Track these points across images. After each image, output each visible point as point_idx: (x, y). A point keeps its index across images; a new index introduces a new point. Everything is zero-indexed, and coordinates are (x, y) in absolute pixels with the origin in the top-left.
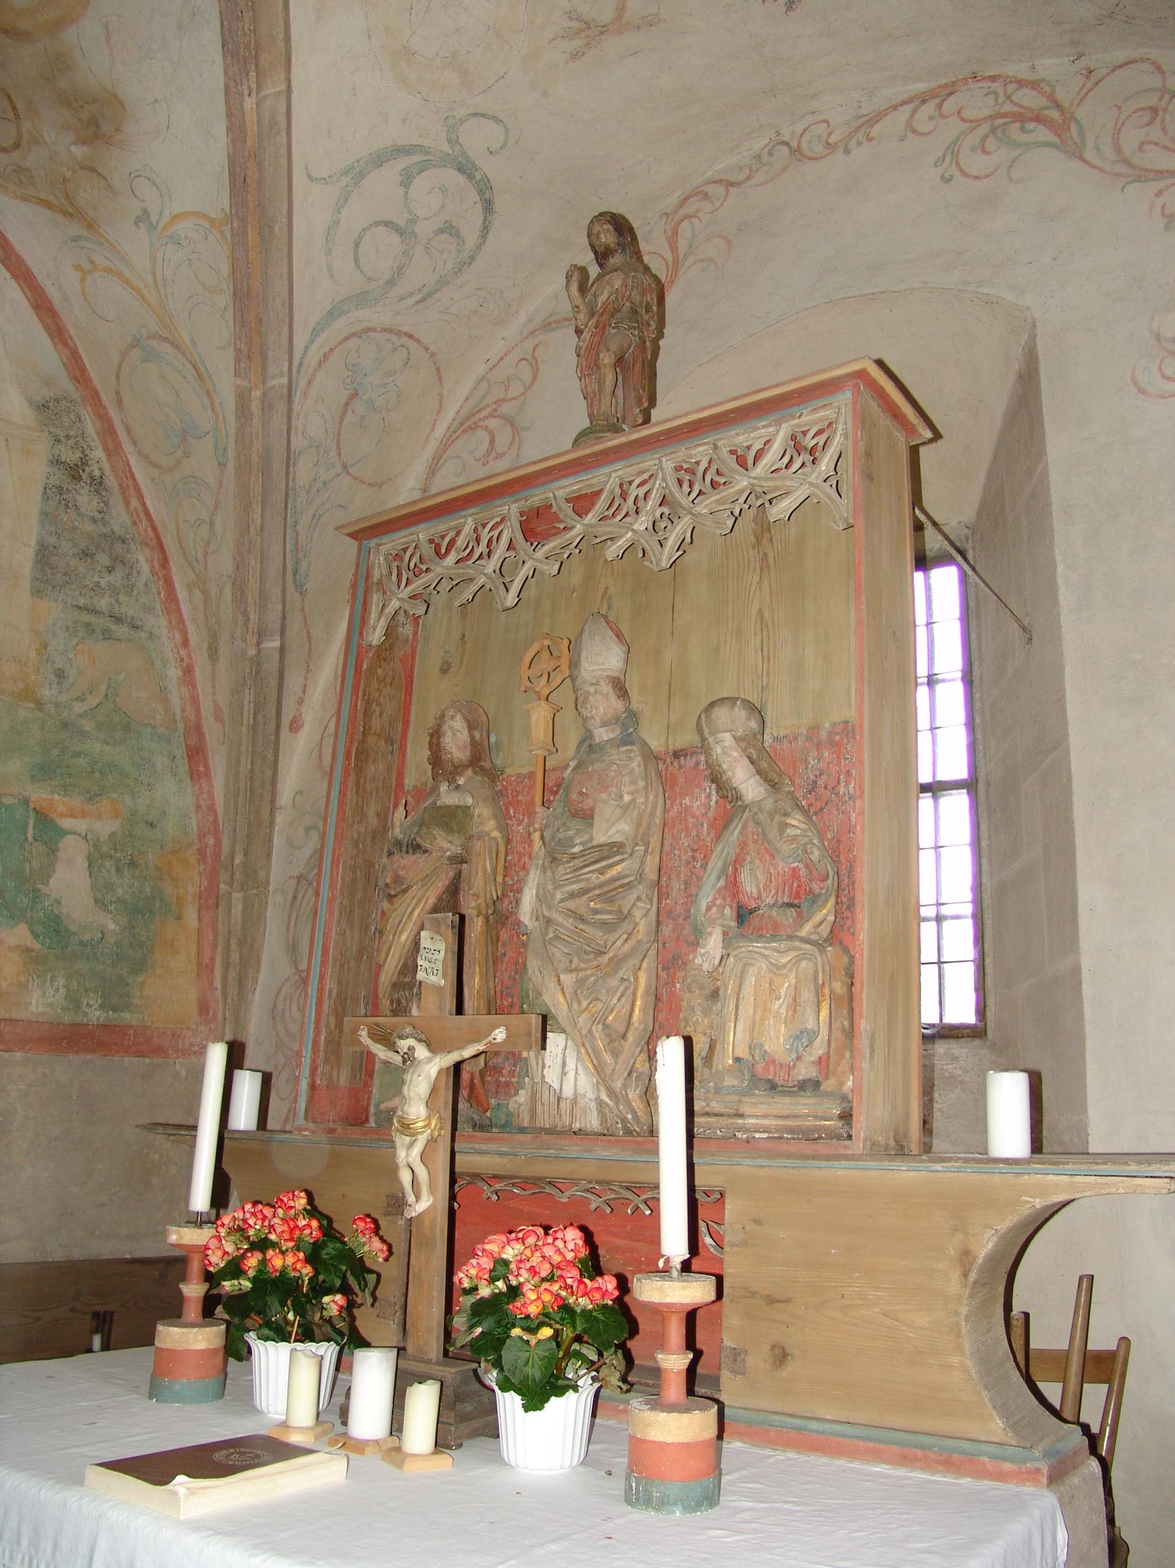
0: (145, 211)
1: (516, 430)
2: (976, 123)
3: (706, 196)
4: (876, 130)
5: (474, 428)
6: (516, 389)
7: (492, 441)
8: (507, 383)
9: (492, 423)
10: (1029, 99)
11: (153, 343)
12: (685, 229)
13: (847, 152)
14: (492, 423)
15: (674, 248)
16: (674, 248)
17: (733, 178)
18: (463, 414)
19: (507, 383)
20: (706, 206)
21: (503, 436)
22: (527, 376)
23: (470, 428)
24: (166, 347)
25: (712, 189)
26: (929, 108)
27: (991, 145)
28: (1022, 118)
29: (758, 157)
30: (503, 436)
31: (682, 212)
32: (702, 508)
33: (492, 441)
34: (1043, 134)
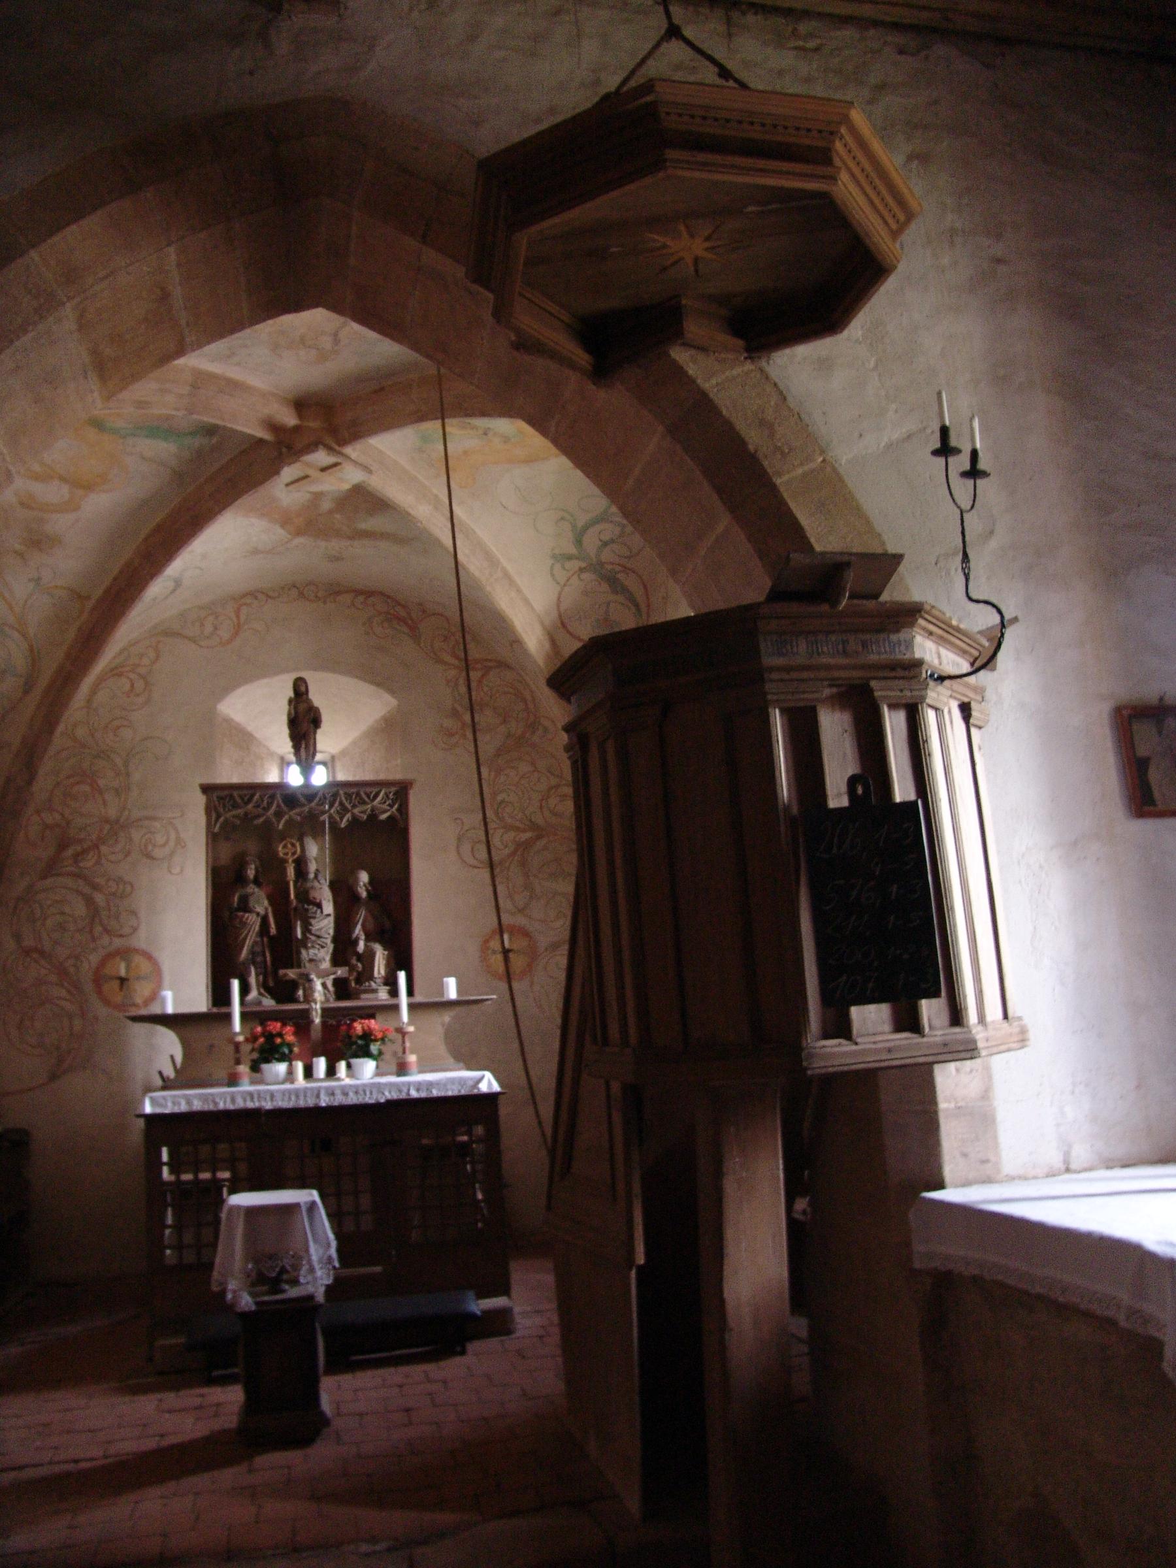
0: (39, 579)
1: (147, 683)
2: (380, 613)
3: (256, 598)
4: (338, 598)
5: (120, 675)
6: (146, 661)
7: (132, 686)
8: (141, 656)
9: (132, 676)
10: (403, 613)
11: (6, 629)
12: (244, 610)
13: (325, 602)
14: (132, 676)
15: (238, 617)
16: (238, 617)
17: (270, 593)
18: (113, 665)
19: (141, 656)
20: (256, 602)
21: (140, 685)
22: (152, 654)
23: (117, 674)
24: (16, 635)
25: (260, 596)
26: (361, 598)
27: (386, 625)
28: (401, 620)
29: (283, 588)
30: (140, 685)
31: (243, 600)
32: (356, 811)
33: (132, 686)
34: (406, 629)
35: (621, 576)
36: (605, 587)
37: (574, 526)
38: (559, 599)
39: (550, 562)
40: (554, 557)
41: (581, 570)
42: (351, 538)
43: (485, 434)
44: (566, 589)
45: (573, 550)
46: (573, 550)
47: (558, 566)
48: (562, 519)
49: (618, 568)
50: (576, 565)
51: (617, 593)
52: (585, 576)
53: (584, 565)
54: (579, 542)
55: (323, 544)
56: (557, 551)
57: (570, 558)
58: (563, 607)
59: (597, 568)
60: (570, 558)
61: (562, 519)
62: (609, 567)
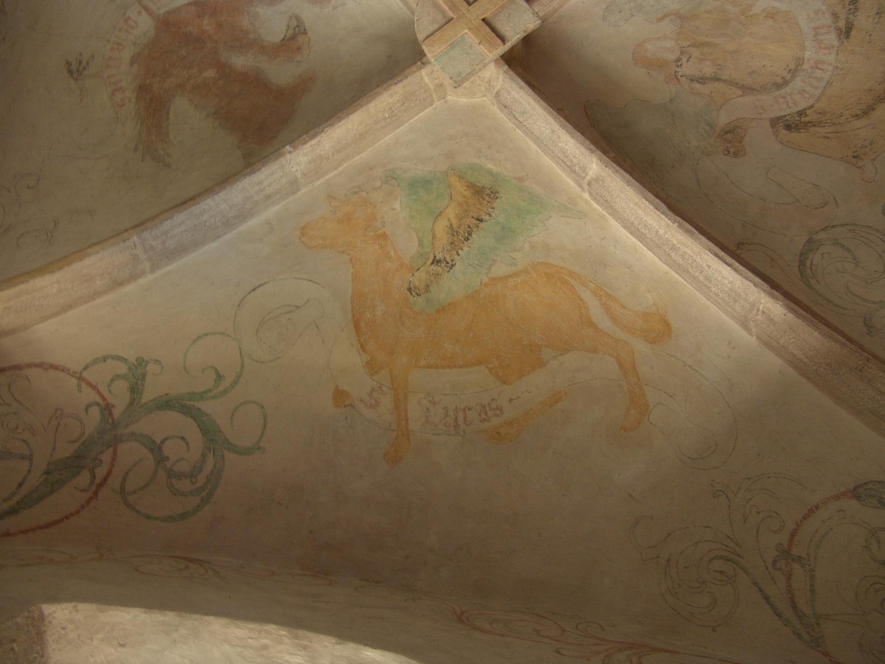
35: (84, 478)
36: (65, 451)
37: (202, 396)
38: (55, 367)
39: (132, 356)
40: (141, 363)
41: (107, 409)
42: (142, 89)
43: (436, 262)
44: (74, 381)
45: (149, 394)
46: (149, 394)
47: (122, 368)
48: (219, 377)
49: (101, 472)
50: (120, 397)
51: (48, 472)
52: (95, 412)
53: (116, 413)
54: (166, 404)
55: (127, 55)
56: (151, 368)
57: (135, 390)
58: (33, 373)
59: (111, 431)
60: (135, 390)
61: (219, 377)
62: (106, 457)
